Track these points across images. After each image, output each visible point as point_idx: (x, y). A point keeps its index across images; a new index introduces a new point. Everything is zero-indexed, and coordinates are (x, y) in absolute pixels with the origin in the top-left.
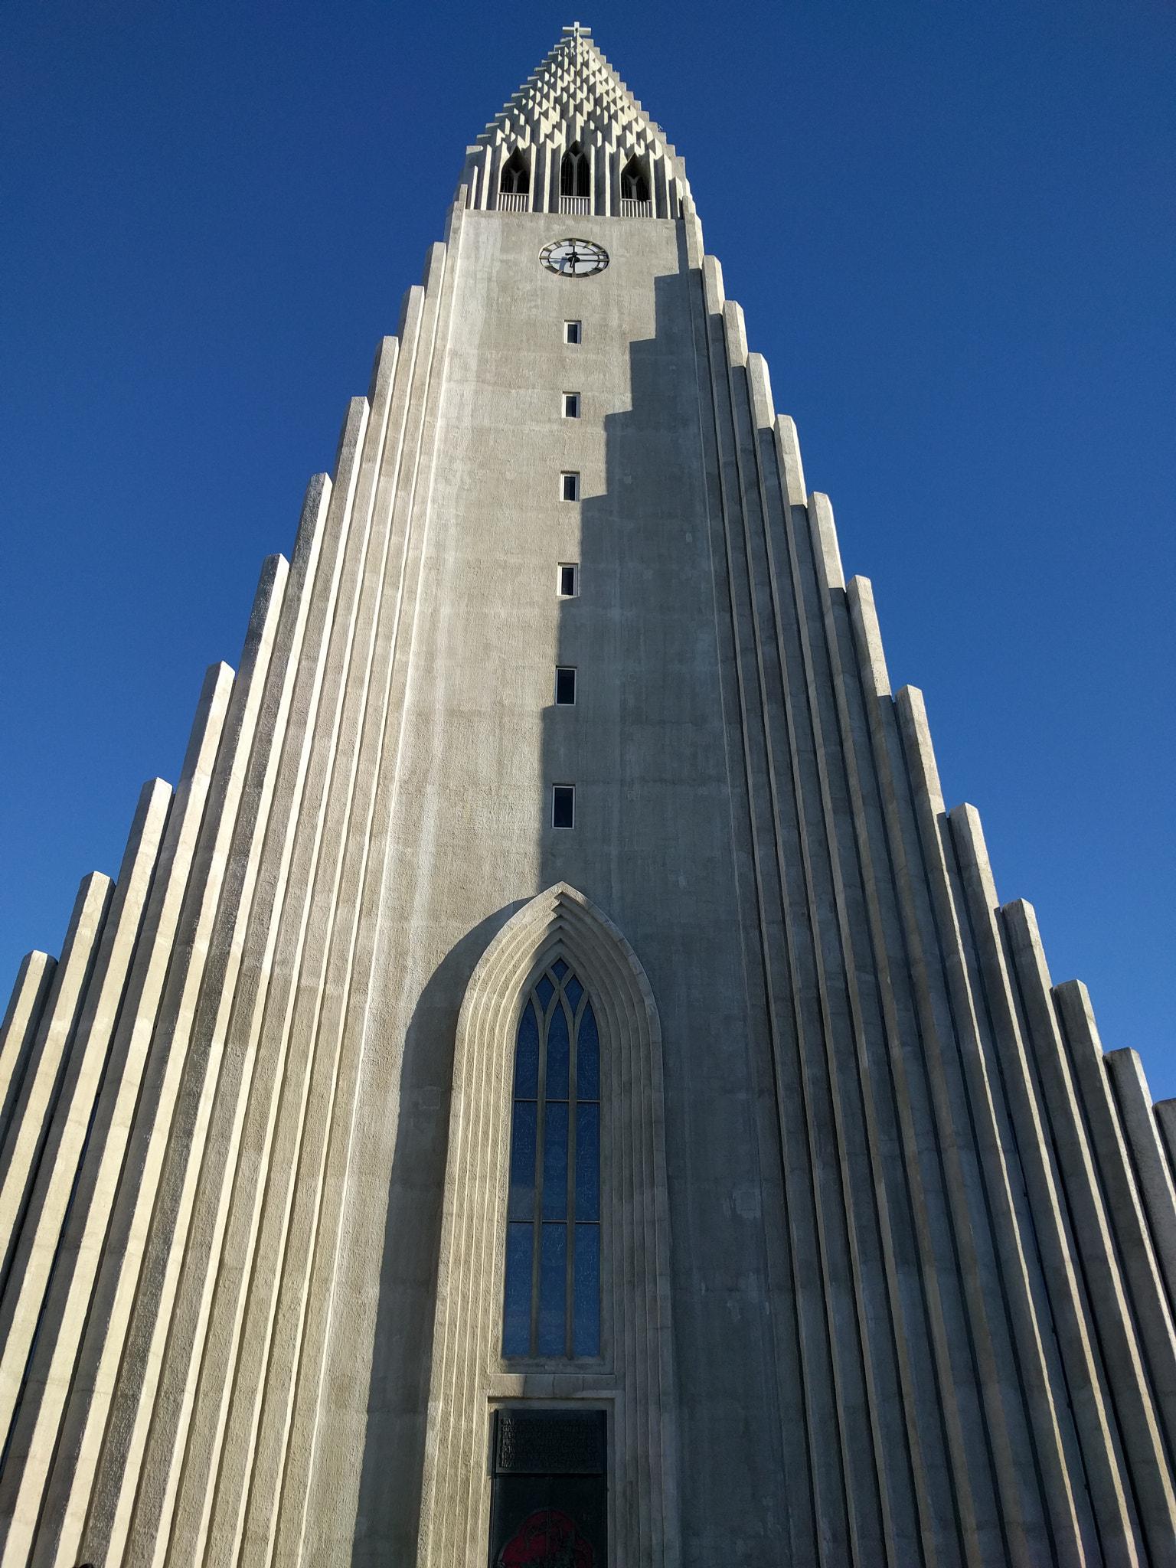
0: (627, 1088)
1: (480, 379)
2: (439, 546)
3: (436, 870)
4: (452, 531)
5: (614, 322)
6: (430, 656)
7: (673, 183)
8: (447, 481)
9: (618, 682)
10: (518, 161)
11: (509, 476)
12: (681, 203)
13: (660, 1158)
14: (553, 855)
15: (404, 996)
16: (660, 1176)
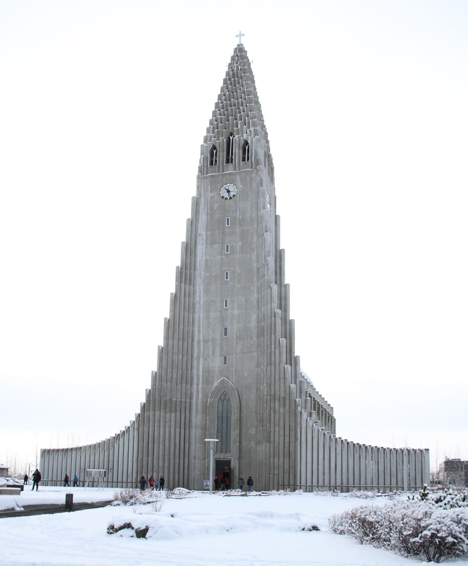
0: (235, 414)
1: (207, 243)
2: (200, 297)
4: (202, 293)
5: (238, 216)
6: (199, 327)
8: (200, 278)
9: (236, 330)
11: (214, 274)
14: (223, 371)
15: (199, 399)
16: (238, 428)
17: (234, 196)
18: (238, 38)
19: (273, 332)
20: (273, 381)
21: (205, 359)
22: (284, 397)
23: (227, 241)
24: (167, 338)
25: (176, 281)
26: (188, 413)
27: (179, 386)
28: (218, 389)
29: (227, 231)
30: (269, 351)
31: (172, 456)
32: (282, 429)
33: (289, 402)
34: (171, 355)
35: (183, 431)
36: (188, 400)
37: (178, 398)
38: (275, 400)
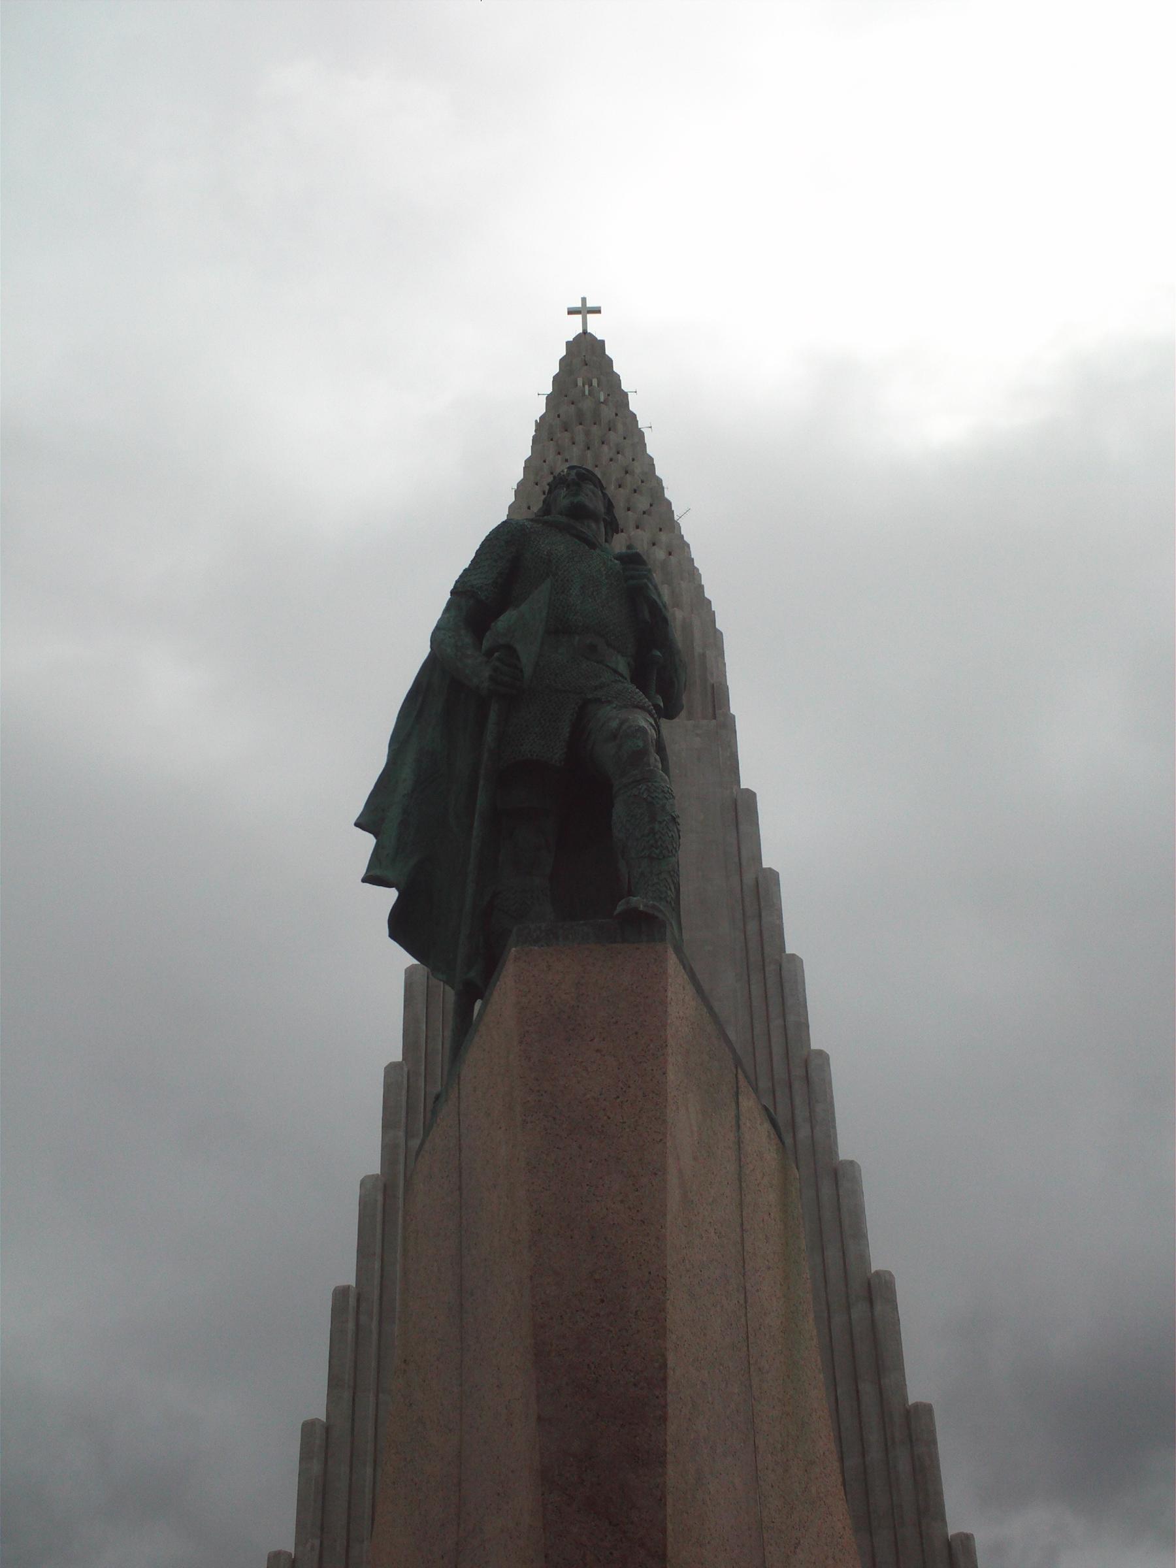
12: (713, 685)
18: (579, 317)
25: (387, 1125)
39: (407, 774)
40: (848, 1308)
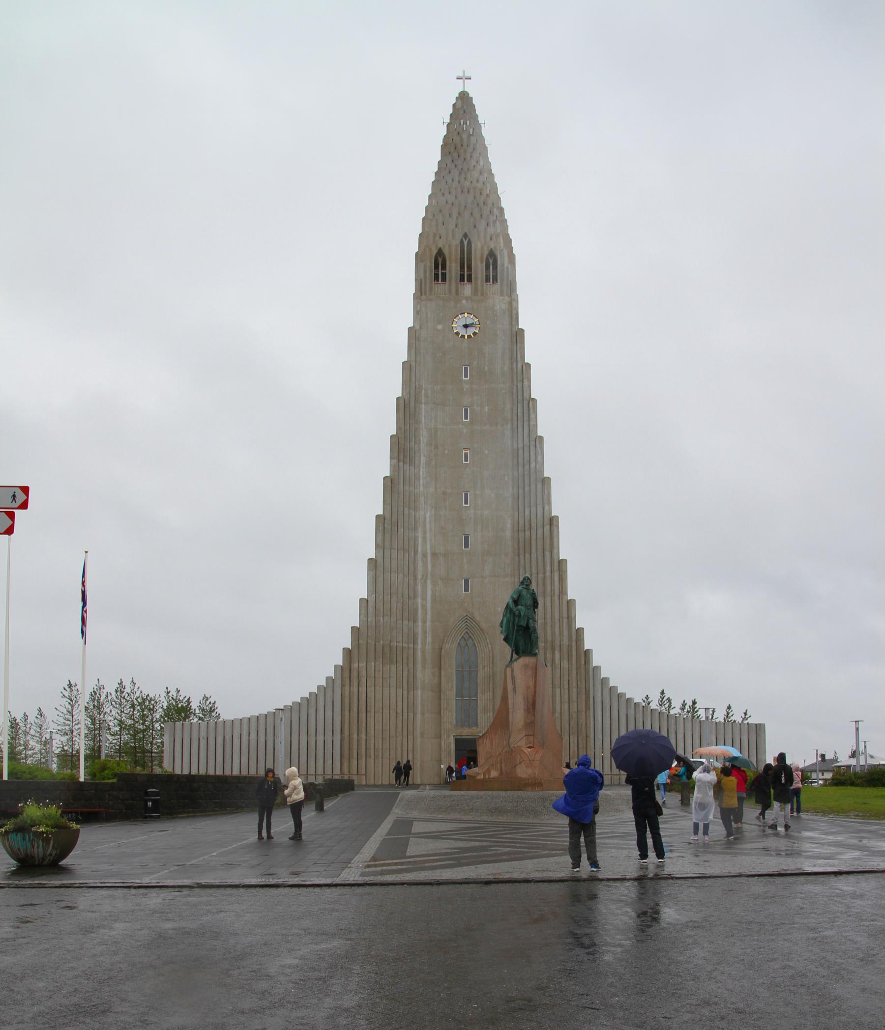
0: (484, 667)
3: (432, 607)
6: (425, 532)
7: (508, 268)
10: (440, 253)
12: (511, 282)
13: (491, 686)
16: (491, 689)
17: (475, 334)
18: (462, 80)
19: (547, 547)
20: (549, 621)
21: (434, 584)
22: (568, 645)
23: (465, 403)
24: (380, 546)
25: (391, 458)
26: (411, 665)
27: (400, 622)
28: (457, 629)
29: (466, 387)
30: (541, 576)
31: (393, 733)
32: (567, 691)
33: (575, 653)
34: (389, 574)
35: (405, 692)
36: (411, 646)
37: (399, 642)
38: (553, 650)
39: (505, 620)
40: (543, 526)
